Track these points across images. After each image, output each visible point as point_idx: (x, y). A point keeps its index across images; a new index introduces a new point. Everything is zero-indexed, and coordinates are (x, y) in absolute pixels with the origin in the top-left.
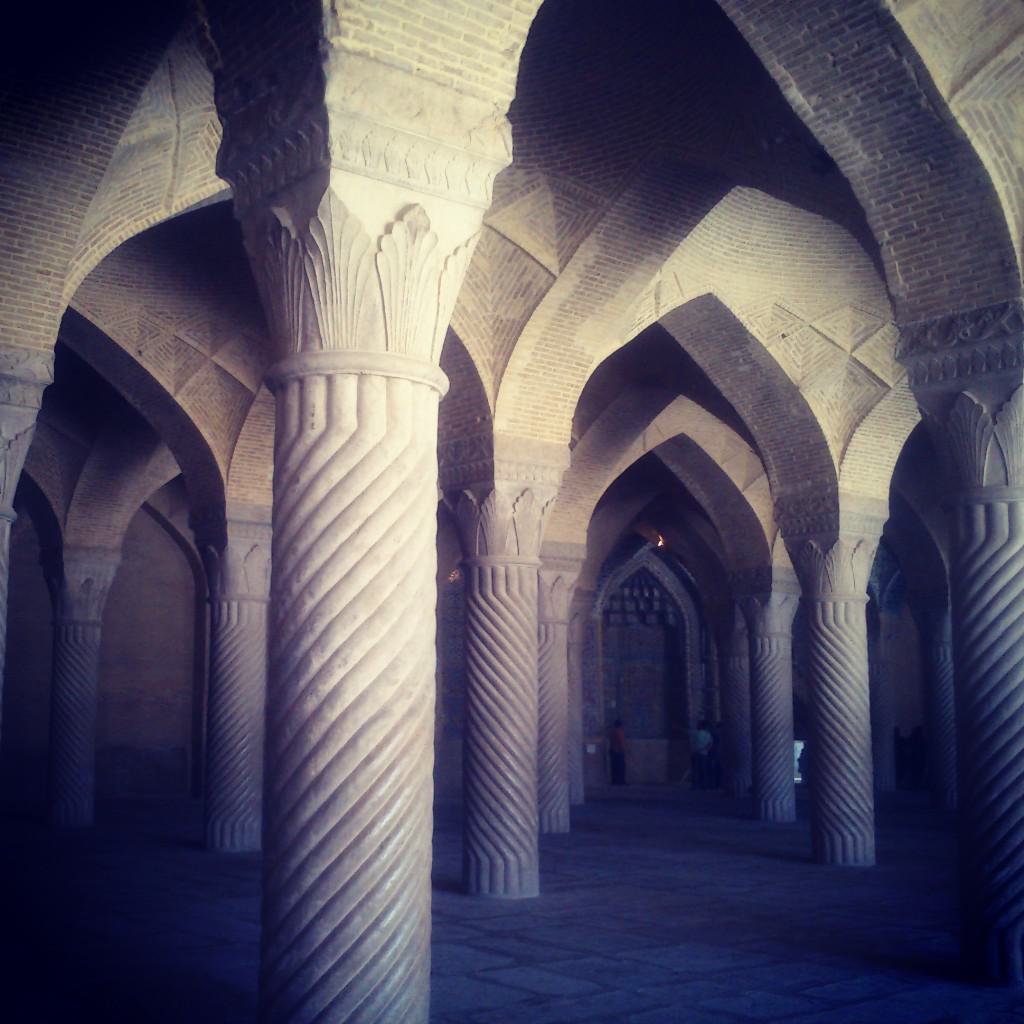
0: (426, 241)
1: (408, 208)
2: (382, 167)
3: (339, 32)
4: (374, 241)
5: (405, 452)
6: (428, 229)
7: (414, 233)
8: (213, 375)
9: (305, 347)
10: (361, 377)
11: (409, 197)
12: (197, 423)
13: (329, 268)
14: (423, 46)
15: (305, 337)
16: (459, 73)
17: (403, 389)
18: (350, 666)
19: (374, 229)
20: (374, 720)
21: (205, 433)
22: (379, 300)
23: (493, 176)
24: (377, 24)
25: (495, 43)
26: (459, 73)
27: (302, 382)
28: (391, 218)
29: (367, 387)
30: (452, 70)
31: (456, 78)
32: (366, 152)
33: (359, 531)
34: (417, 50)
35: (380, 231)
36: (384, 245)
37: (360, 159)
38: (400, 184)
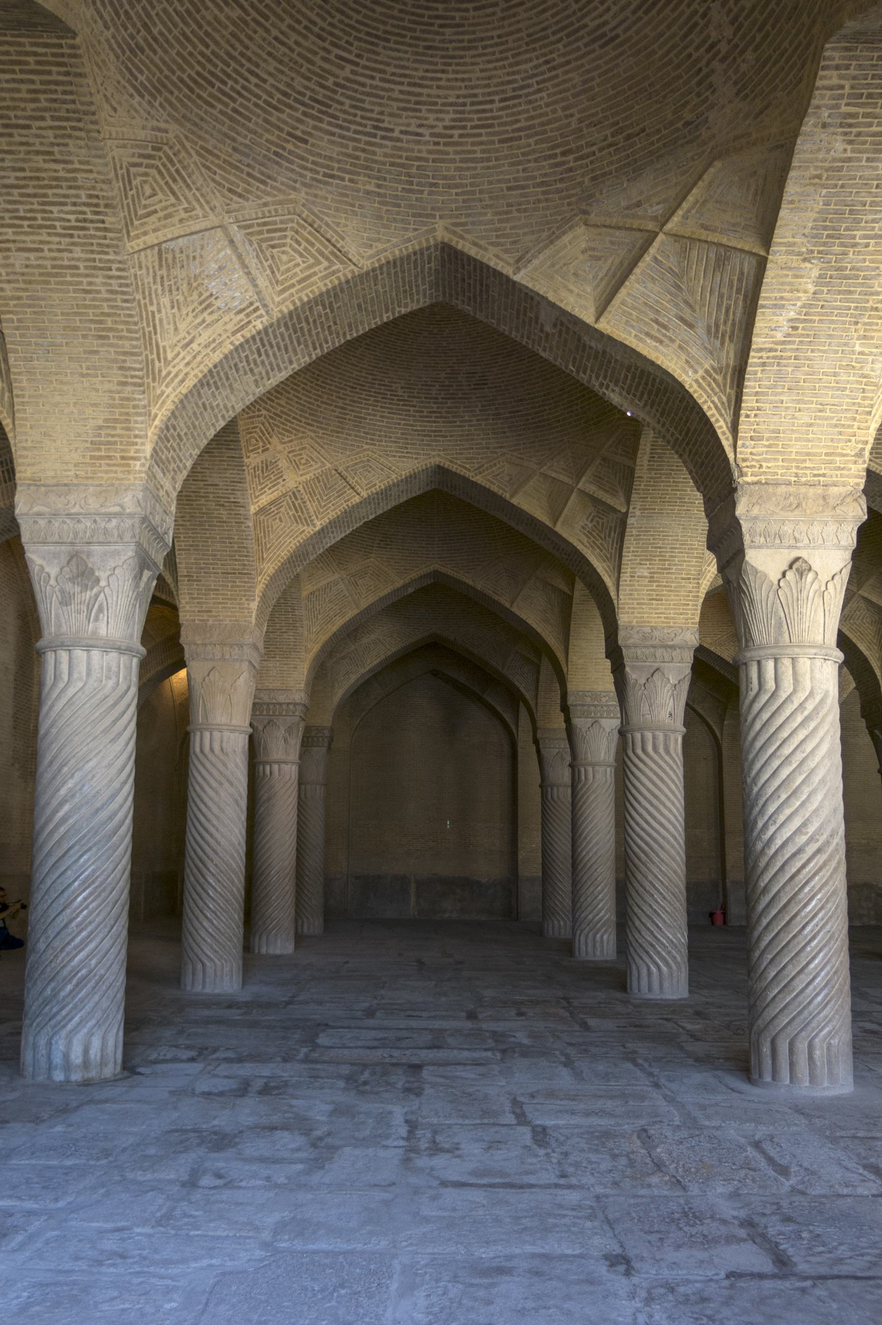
0: (811, 576)
1: (797, 559)
2: (778, 541)
3: (742, 475)
4: (776, 582)
5: (806, 699)
6: (810, 569)
7: (801, 574)
8: (863, 605)
9: (746, 646)
10: (776, 660)
11: (795, 554)
12: (854, 640)
13: (752, 602)
14: (797, 467)
15: (747, 641)
16: (824, 475)
17: (804, 664)
18: (778, 825)
19: (774, 576)
20: (794, 855)
21: (862, 647)
22: (782, 615)
23: (856, 529)
24: (764, 464)
25: (849, 451)
26: (824, 475)
27: (745, 664)
28: (785, 567)
29: (780, 665)
30: (819, 475)
31: (821, 479)
32: (766, 534)
33: (778, 748)
34: (794, 470)
35: (780, 576)
36: (782, 584)
37: (762, 540)
38: (789, 547)
